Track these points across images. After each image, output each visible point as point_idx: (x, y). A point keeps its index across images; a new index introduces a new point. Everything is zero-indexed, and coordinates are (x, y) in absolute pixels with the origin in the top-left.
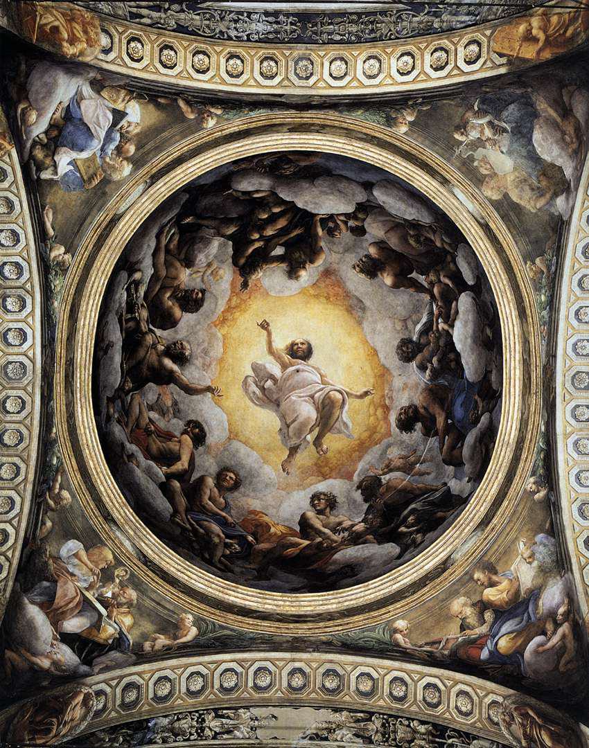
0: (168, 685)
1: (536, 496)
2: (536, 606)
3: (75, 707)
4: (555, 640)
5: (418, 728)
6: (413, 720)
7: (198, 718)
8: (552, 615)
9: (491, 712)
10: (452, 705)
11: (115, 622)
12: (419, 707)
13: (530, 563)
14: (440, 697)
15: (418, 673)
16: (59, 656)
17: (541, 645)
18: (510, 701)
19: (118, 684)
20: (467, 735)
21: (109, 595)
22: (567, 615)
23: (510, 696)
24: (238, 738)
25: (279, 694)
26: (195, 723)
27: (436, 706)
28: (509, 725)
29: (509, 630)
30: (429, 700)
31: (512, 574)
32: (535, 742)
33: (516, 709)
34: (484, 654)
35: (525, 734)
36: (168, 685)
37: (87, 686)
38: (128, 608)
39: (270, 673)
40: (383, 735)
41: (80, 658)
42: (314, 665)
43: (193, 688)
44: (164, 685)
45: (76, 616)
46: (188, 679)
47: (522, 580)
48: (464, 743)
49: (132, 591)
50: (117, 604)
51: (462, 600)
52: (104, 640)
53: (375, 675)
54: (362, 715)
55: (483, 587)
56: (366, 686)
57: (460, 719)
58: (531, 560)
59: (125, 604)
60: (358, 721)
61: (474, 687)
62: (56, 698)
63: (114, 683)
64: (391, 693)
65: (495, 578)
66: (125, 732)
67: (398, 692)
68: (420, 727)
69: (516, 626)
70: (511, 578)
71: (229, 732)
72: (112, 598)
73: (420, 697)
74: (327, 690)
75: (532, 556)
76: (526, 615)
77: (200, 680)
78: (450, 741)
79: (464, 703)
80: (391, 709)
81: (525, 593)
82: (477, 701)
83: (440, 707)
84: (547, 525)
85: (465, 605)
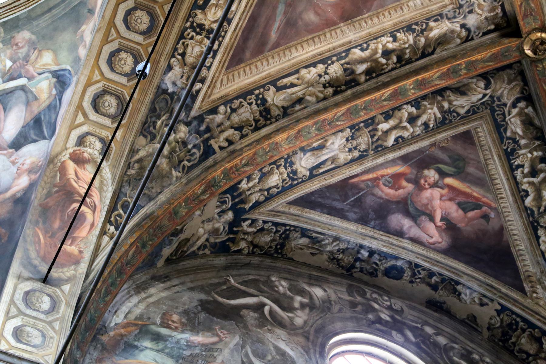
0: (123, 55)
3: (77, 175)
7: (194, 31)
11: (40, 74)
16: (28, 162)
19: (85, 115)
21: (9, 64)
26: (199, 37)
36: (123, 55)
37: (60, 153)
38: (35, 49)
41: (44, 138)
43: (144, 27)
44: (120, 60)
45: (6, 117)
46: (128, 28)
49: (20, 34)
50: (23, 60)
52: (49, 97)
59: (29, 51)
62: (49, 195)
63: (80, 119)
66: (162, 123)
72: (14, 62)
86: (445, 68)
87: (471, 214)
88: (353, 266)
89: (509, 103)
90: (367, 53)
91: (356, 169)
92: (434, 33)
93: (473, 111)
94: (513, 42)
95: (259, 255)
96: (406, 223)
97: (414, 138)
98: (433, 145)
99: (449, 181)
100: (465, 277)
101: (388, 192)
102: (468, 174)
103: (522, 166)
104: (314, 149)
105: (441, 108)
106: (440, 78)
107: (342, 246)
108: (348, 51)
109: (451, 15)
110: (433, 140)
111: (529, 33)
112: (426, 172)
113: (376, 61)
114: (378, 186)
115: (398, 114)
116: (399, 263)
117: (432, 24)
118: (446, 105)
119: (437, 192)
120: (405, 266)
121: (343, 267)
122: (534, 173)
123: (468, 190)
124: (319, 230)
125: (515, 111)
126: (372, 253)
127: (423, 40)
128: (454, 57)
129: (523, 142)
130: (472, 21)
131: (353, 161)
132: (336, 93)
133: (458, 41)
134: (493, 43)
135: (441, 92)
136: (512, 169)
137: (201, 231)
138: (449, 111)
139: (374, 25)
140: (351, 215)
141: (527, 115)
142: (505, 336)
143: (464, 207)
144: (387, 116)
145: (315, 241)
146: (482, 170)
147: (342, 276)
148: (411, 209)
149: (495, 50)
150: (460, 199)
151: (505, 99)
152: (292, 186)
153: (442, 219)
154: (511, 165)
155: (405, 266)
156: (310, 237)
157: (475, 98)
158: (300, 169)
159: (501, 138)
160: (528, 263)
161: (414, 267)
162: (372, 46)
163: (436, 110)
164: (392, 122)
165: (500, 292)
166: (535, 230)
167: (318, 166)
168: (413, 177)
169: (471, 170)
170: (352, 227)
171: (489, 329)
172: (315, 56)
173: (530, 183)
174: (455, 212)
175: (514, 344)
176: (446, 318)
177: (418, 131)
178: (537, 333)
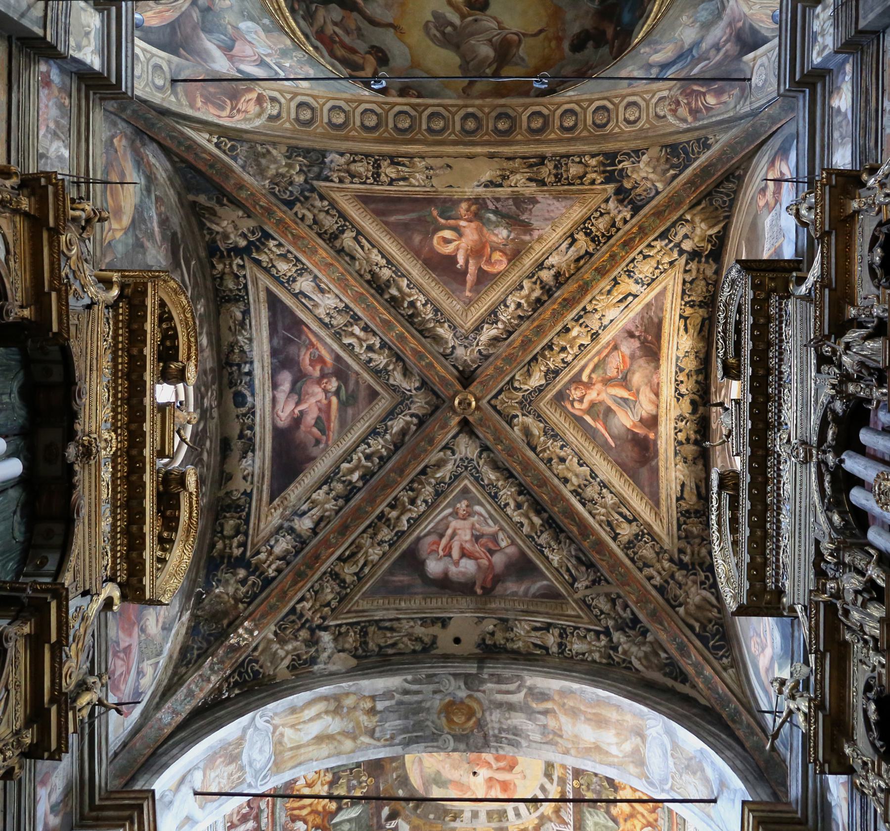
10: (621, 118)
12: (589, 131)
15: (586, 100)
24: (414, 186)
25: (453, 137)
30: (598, 122)
39: (443, 118)
40: (556, 176)
53: (545, 112)
56: (537, 124)
60: (531, 166)
64: (562, 126)
67: (569, 122)
71: (404, 179)
73: (589, 121)
77: (375, 117)
78: (620, 166)
86: (420, 349)
87: (315, 430)
88: (231, 365)
89: (412, 411)
90: (407, 290)
91: (314, 326)
92: (440, 331)
93: (395, 389)
94: (459, 387)
95: (214, 285)
96: (286, 386)
97: (356, 357)
98: (357, 374)
99: (334, 400)
100: (261, 453)
101: (305, 358)
102: (346, 411)
103: (369, 446)
104: (318, 286)
105: (387, 365)
106: (412, 349)
107: (246, 348)
108: (403, 276)
109: (458, 334)
110: (361, 371)
111: (471, 393)
112: (334, 379)
113: (403, 299)
114: (308, 349)
115: (370, 335)
116: (250, 399)
117: (446, 325)
118: (391, 367)
119: (321, 396)
120: (249, 405)
121: (228, 356)
122: (368, 457)
123: (333, 418)
124: (253, 323)
125: (408, 418)
126: (250, 373)
127: (432, 325)
128: (430, 353)
129: (388, 437)
130: (460, 352)
131: (320, 320)
132: (368, 282)
133: (441, 350)
134: (451, 374)
135: (399, 358)
136: (364, 440)
137: (225, 223)
138: (387, 372)
139: (429, 284)
140: (275, 341)
141: (409, 428)
142: (228, 508)
143: (318, 422)
144: (366, 329)
145: (242, 324)
146: (353, 420)
147: (219, 360)
148: (299, 384)
149: (449, 377)
150: (323, 416)
151: (413, 406)
152: (282, 283)
153: (301, 412)
154: (367, 438)
155: (249, 405)
156: (244, 319)
157: (405, 385)
158: (298, 283)
159: (384, 420)
160: (296, 492)
161: (252, 412)
162: (413, 291)
163: (385, 361)
164: (362, 334)
165: (262, 485)
166: (325, 483)
167: (306, 296)
168: (326, 371)
169: (350, 411)
170: (266, 347)
171: (227, 493)
172: (390, 254)
173: (359, 460)
174: (310, 419)
175: (225, 517)
176: (219, 458)
177: (364, 357)
178: (243, 528)
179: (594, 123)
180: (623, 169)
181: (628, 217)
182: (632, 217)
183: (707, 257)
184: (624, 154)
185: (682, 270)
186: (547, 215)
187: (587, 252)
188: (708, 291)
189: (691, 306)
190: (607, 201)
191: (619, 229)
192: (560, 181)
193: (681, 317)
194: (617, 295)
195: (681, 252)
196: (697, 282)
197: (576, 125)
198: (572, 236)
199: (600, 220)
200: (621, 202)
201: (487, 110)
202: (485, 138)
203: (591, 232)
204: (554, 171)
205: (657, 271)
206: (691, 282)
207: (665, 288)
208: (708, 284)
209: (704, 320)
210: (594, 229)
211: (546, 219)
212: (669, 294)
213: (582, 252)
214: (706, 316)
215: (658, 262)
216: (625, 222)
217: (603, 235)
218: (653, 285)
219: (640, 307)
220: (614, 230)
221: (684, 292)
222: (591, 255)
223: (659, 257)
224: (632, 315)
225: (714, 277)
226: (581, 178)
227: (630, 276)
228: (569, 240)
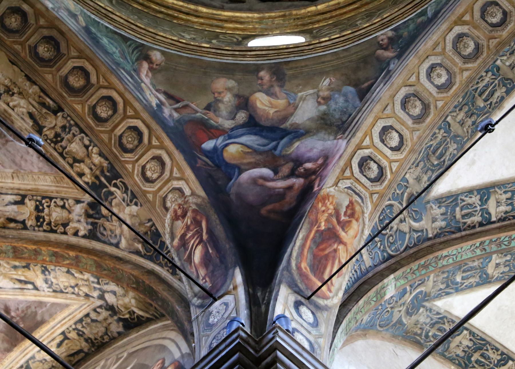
1: (380, 52)
2: (290, 143)
4: (280, 184)
5: (93, 155)
6: (95, 146)
8: (298, 162)
9: (170, 196)
12: (110, 139)
13: (319, 103)
14: (137, 147)
15: (135, 110)
17: (265, 179)
18: (194, 200)
20: (134, 196)
22: (308, 174)
23: (199, 196)
27: (126, 151)
28: (176, 217)
29: (248, 143)
30: (124, 141)
31: (295, 100)
32: (186, 249)
33: (194, 211)
34: (209, 145)
35: (183, 236)
40: (57, 135)
42: (42, 22)
47: (299, 112)
48: (124, 200)
51: (231, 83)
53: (93, 79)
54: (51, 102)
55: (260, 88)
56: (77, 82)
57: (138, 179)
58: (322, 101)
60: (43, 105)
61: (174, 163)
65: (277, 89)
67: (103, 112)
68: (96, 156)
69: (258, 145)
70: (292, 102)
73: (118, 131)
74: (37, 54)
75: (327, 99)
76: (274, 143)
78: (113, 189)
79: (153, 169)
80: (82, 119)
81: (292, 125)
82: (166, 178)
83: (129, 155)
84: (366, 85)
85: (229, 89)
179: (121, 137)
180: (112, 193)
181: (81, 233)
182: (84, 237)
183: (120, 320)
184: (124, 183)
185: (93, 306)
186: (18, 159)
187: (23, 222)
188: (102, 337)
189: (79, 335)
190: (78, 201)
191: (65, 233)
192: (56, 143)
193: (63, 333)
194: (21, 274)
195: (101, 297)
196: (99, 325)
197: (105, 120)
198: (24, 197)
199: (59, 210)
200: (88, 216)
201: (42, 22)
202: (18, 47)
203: (42, 211)
204: (59, 130)
205: (70, 290)
206: (93, 321)
207: (67, 306)
208: (106, 334)
209: (80, 351)
210: (46, 210)
211: (14, 162)
212: (66, 312)
213: (20, 218)
214: (86, 350)
215: (77, 285)
216: (76, 234)
217: (49, 224)
218: (59, 295)
219: (33, 298)
220: (61, 229)
221: (81, 321)
222: (25, 228)
223: (80, 283)
224: (21, 298)
225: (115, 335)
226: (76, 160)
227: (43, 272)
228: (18, 198)
